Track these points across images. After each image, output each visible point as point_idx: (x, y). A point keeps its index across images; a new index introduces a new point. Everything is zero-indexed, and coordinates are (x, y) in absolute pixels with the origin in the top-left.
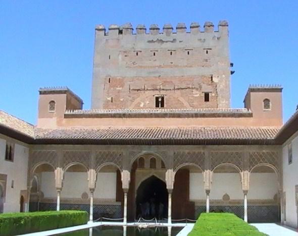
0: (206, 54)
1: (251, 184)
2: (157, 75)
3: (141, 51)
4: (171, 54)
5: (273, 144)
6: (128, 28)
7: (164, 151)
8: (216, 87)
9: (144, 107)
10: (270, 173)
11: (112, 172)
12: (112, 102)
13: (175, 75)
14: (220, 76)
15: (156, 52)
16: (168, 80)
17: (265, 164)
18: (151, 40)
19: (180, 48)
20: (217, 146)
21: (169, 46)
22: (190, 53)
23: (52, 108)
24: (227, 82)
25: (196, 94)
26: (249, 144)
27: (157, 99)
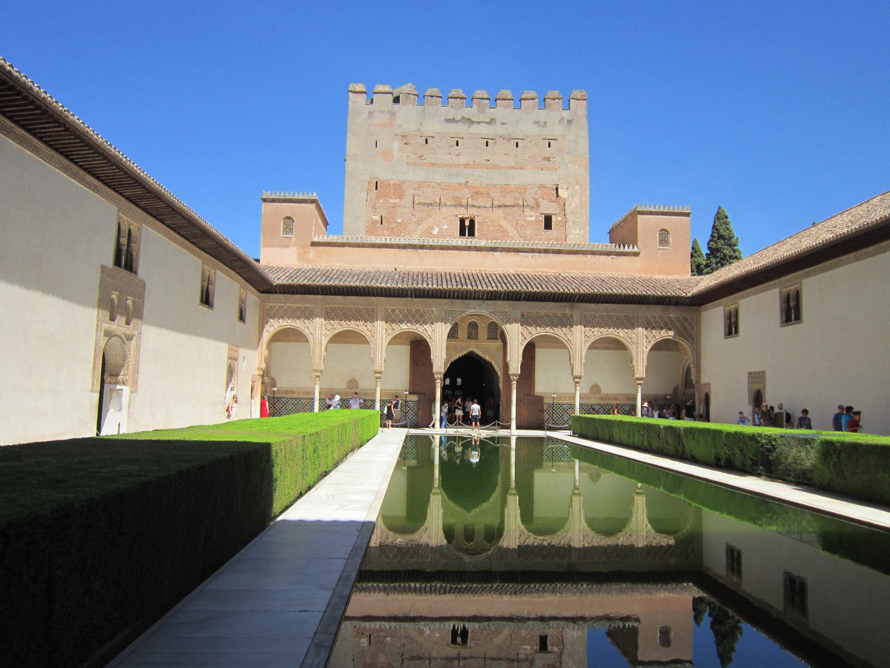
0: (548, 149)
2: (462, 180)
3: (433, 137)
4: (487, 145)
5: (686, 305)
6: (409, 94)
7: (506, 310)
8: (564, 206)
10: (668, 353)
11: (401, 344)
12: (382, 223)
13: (495, 182)
14: (570, 188)
16: (482, 191)
18: (451, 118)
20: (593, 305)
22: (519, 145)
23: (288, 229)
24: (584, 198)
25: (531, 216)
26: (647, 303)
27: (462, 221)
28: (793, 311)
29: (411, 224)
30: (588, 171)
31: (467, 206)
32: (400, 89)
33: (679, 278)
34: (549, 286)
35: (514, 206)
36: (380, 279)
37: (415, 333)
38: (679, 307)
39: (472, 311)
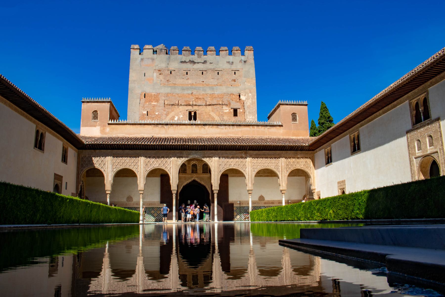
0: (234, 75)
1: (287, 185)
2: (190, 92)
4: (203, 74)
5: (306, 150)
8: (244, 104)
9: (178, 119)
10: (300, 177)
11: (155, 176)
12: (147, 115)
13: (207, 93)
14: (246, 95)
15: (188, 71)
16: (200, 97)
17: (299, 168)
18: (184, 61)
19: (210, 69)
21: (201, 66)
22: (219, 73)
25: (227, 110)
27: (190, 113)
28: (356, 146)
29: (163, 115)
30: (255, 86)
31: (193, 105)
32: (157, 47)
33: (303, 138)
34: (233, 142)
35: (217, 105)
36: (142, 141)
37: (163, 170)
38: (303, 151)
39: (191, 157)
